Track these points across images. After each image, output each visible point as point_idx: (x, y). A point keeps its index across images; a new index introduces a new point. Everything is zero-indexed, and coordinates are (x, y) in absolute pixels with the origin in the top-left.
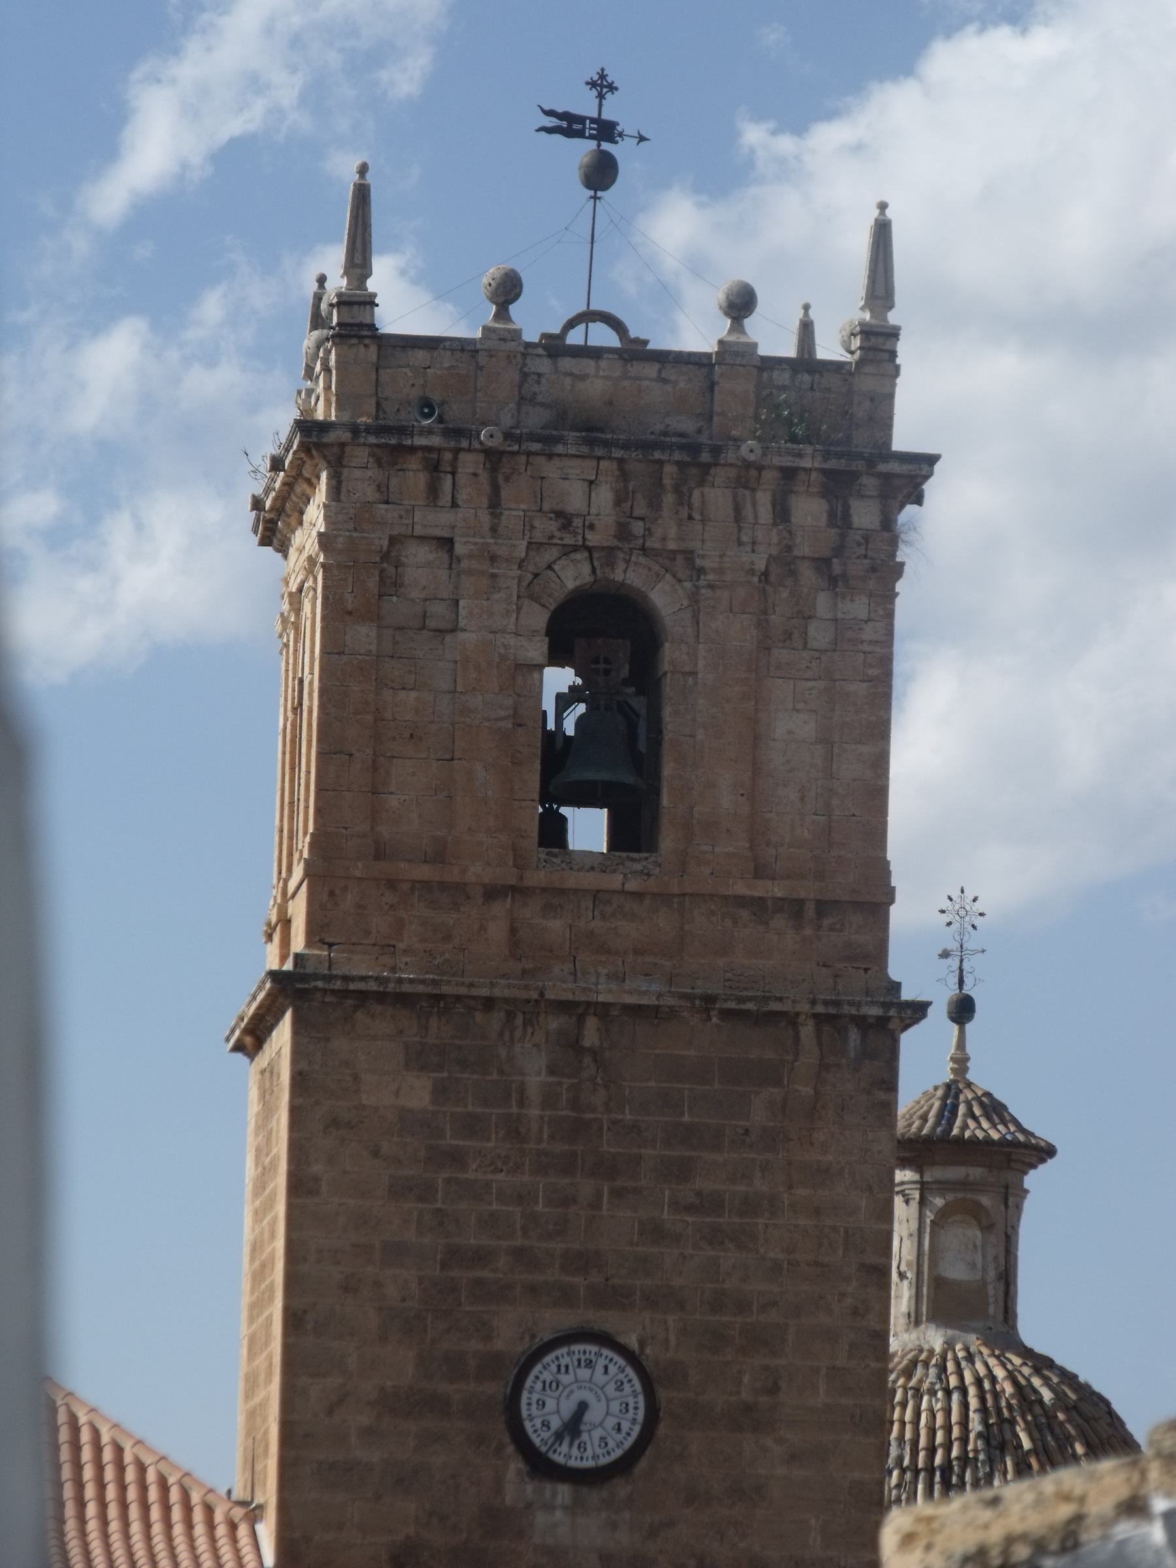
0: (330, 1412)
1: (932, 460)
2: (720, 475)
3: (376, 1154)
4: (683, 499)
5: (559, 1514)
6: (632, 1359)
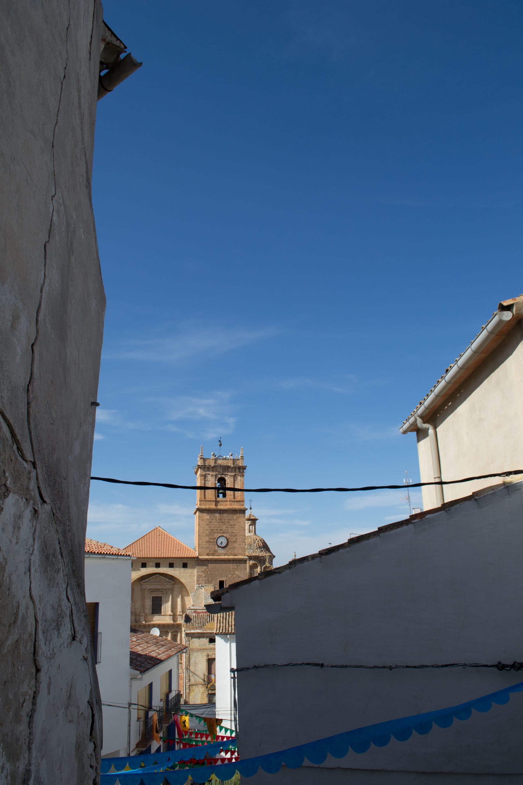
0: (202, 543)
1: (246, 466)
2: (230, 468)
3: (205, 522)
4: (227, 470)
5: (220, 550)
6: (226, 538)
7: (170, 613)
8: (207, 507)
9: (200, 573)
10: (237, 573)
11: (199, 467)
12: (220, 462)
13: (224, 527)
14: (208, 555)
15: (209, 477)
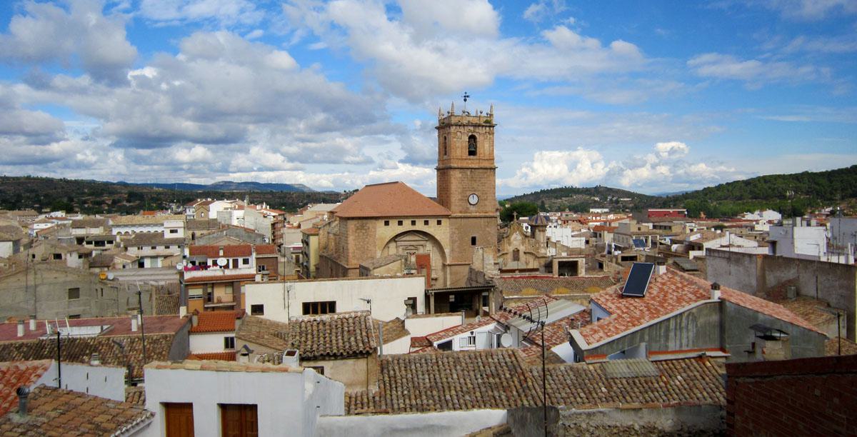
9: (454, 230)
10: (487, 229)
13: (475, 185)
14: (461, 212)
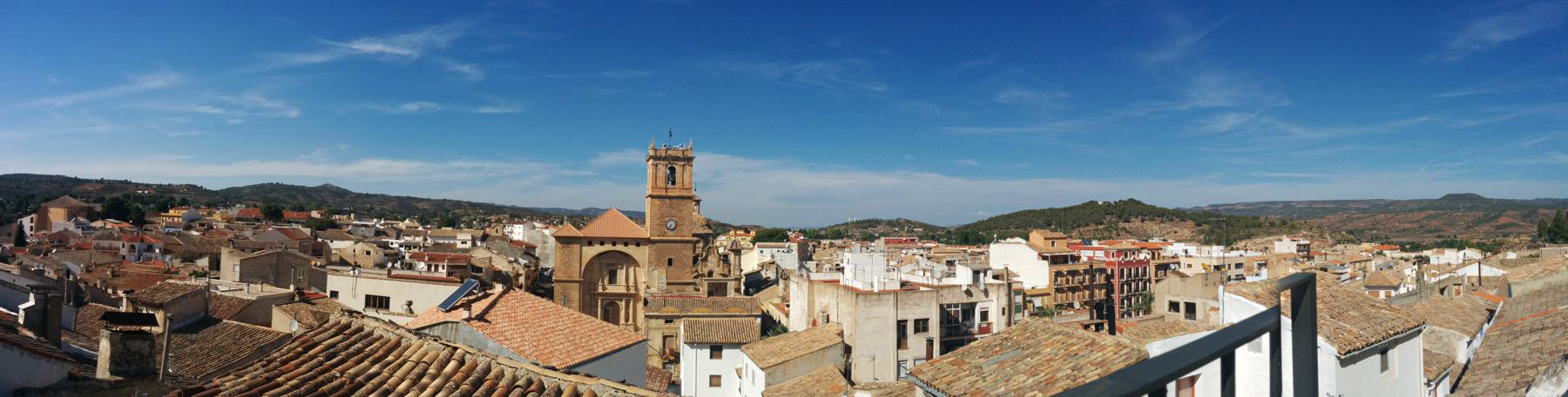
7: (624, 284)
8: (659, 194)
10: (684, 252)
11: (651, 157)
12: (670, 152)
13: (673, 212)
14: (659, 236)
15: (659, 166)
